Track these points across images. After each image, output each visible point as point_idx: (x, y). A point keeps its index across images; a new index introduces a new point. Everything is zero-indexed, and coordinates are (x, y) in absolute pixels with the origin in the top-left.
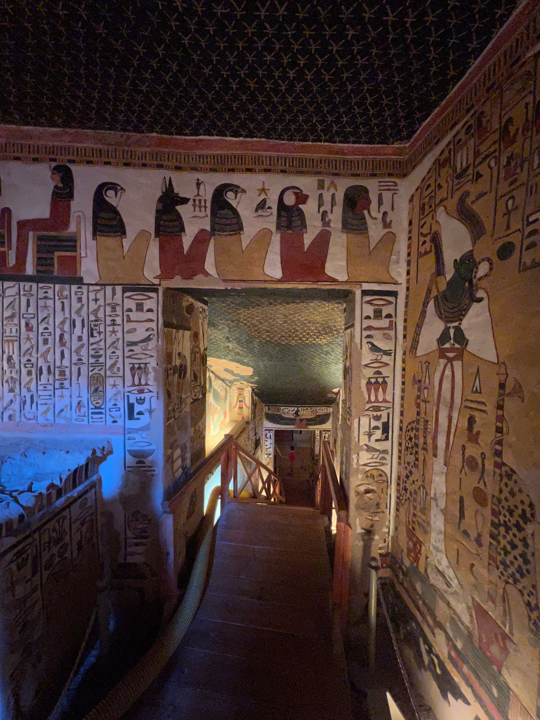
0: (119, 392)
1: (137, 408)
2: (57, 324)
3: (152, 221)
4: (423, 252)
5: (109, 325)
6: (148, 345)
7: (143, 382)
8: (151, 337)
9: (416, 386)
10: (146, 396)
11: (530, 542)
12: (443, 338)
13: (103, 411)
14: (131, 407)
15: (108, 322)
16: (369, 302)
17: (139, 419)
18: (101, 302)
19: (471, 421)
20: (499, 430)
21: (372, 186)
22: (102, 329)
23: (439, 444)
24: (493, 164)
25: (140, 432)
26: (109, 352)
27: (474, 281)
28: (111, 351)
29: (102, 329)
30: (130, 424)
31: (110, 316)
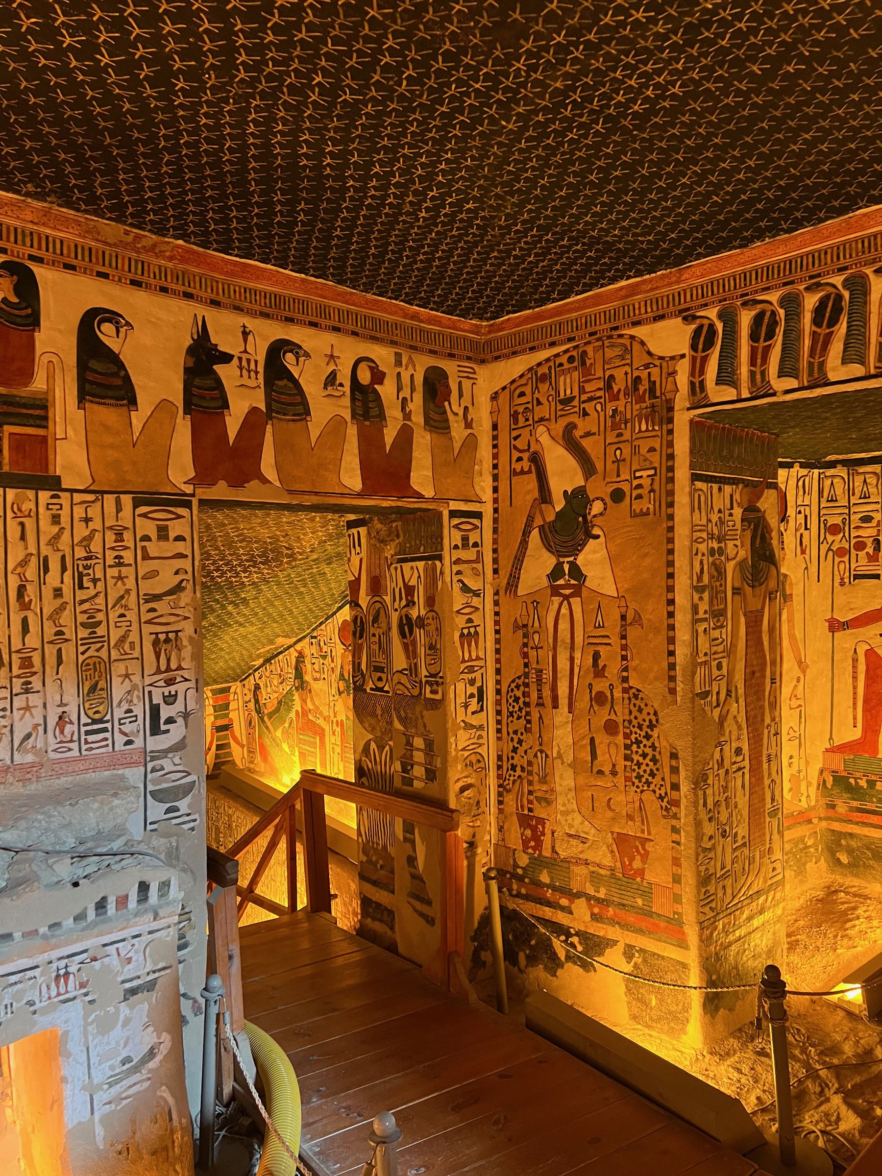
0: (135, 687)
1: (165, 712)
2: (10, 567)
3: (179, 386)
4: (518, 470)
5: (110, 566)
6: (179, 598)
7: (173, 666)
8: (183, 584)
9: (520, 633)
10: (180, 688)
11: (657, 745)
12: (556, 573)
13: (109, 725)
14: (155, 711)
15: (110, 561)
16: (456, 527)
17: (168, 731)
18: (96, 524)
19: (596, 656)
20: (624, 658)
21: (450, 367)
22: (99, 575)
23: (560, 692)
24: (599, 407)
25: (170, 755)
26: (113, 616)
27: (589, 518)
28: (117, 614)
29: (99, 575)
30: (156, 743)
31: (112, 548)
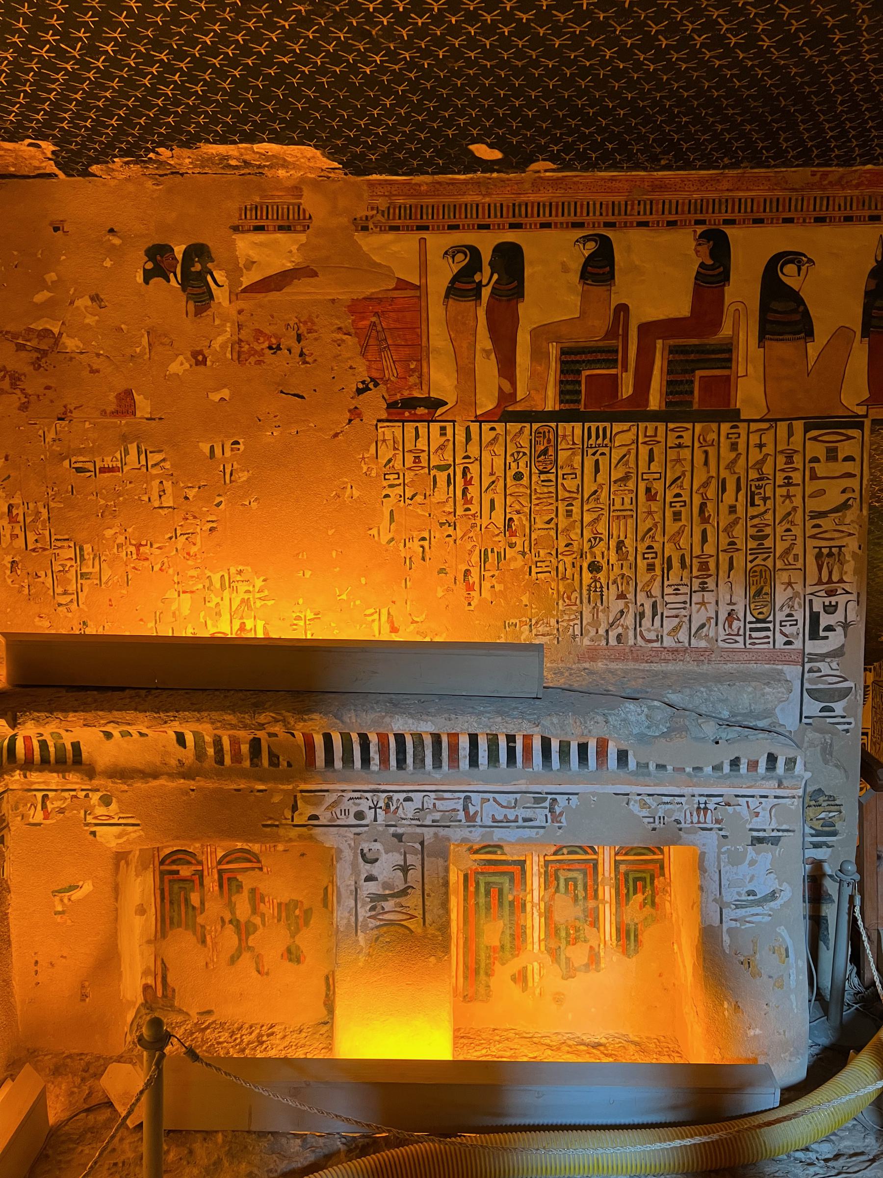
0: (797, 594)
1: (825, 620)
2: (695, 488)
3: (858, 311)
5: (779, 486)
6: (845, 516)
7: (835, 578)
8: (850, 502)
10: (841, 599)
13: (771, 625)
14: (815, 618)
15: (779, 482)
17: (826, 638)
18: (769, 449)
22: (769, 494)
25: (828, 660)
26: (780, 530)
28: (784, 528)
29: (769, 494)
30: (812, 647)
31: (782, 470)
